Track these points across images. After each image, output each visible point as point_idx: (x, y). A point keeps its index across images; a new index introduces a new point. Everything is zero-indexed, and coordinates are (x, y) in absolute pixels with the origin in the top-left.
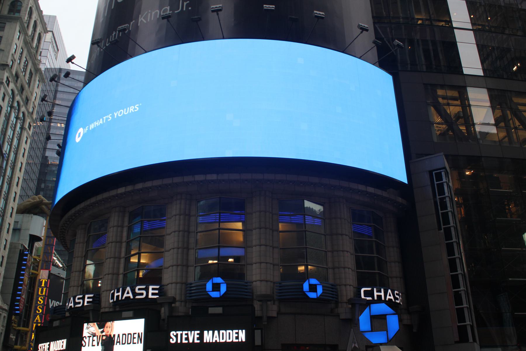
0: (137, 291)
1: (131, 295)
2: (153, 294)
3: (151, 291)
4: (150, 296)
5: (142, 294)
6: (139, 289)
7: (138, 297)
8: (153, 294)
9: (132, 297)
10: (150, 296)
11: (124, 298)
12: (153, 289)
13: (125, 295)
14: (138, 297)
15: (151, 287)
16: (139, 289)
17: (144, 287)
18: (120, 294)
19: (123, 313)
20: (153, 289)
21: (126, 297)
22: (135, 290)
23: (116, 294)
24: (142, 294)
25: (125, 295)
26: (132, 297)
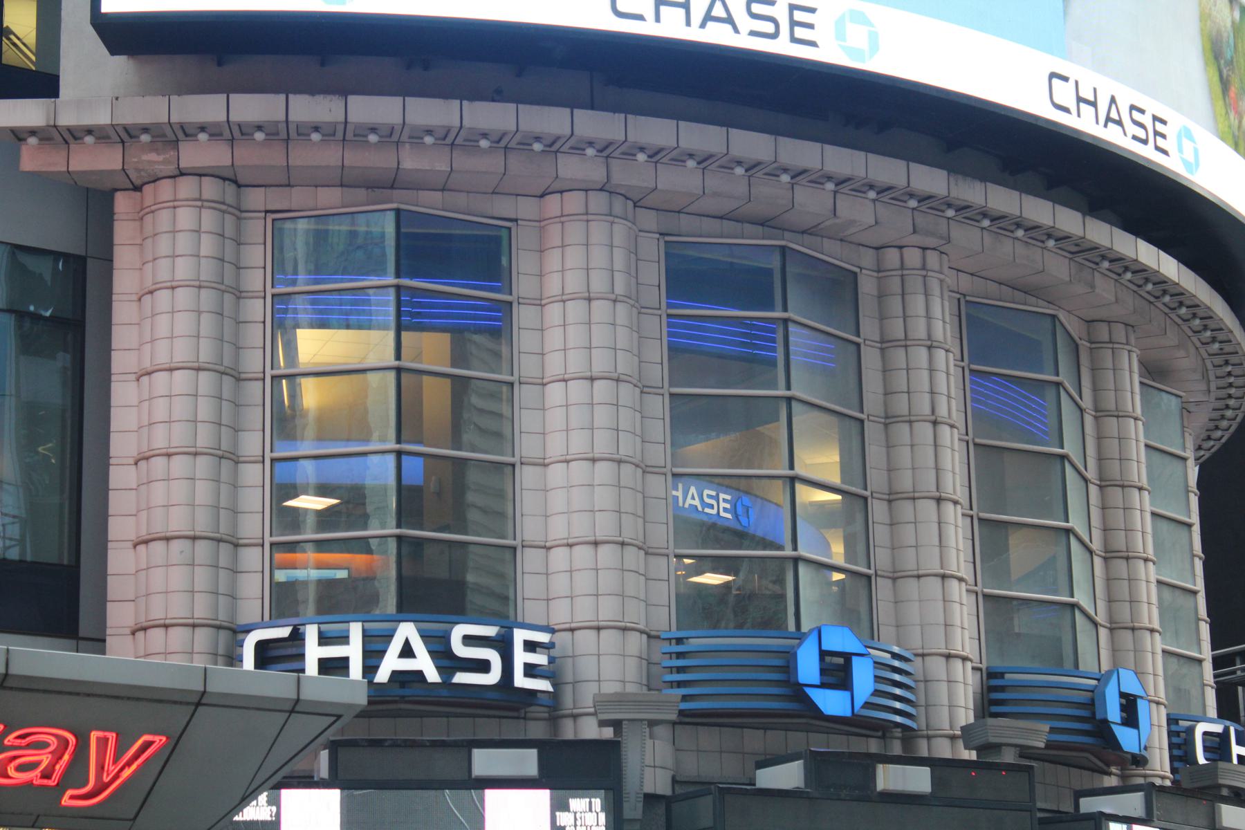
0: (460, 650)
1: (424, 663)
2: (530, 671)
3: (521, 657)
4: (520, 681)
5: (483, 666)
6: (469, 640)
7: (461, 678)
8: (530, 671)
9: (432, 675)
10: (520, 681)
11: (382, 676)
12: (530, 646)
13: (391, 663)
14: (461, 678)
15: (520, 636)
16: (469, 640)
17: (490, 631)
18: (354, 651)
19: (477, 754)
20: (530, 646)
21: (395, 674)
22: (446, 638)
23: (314, 652)
24: (483, 666)
25: (391, 663)
26: (432, 675)
